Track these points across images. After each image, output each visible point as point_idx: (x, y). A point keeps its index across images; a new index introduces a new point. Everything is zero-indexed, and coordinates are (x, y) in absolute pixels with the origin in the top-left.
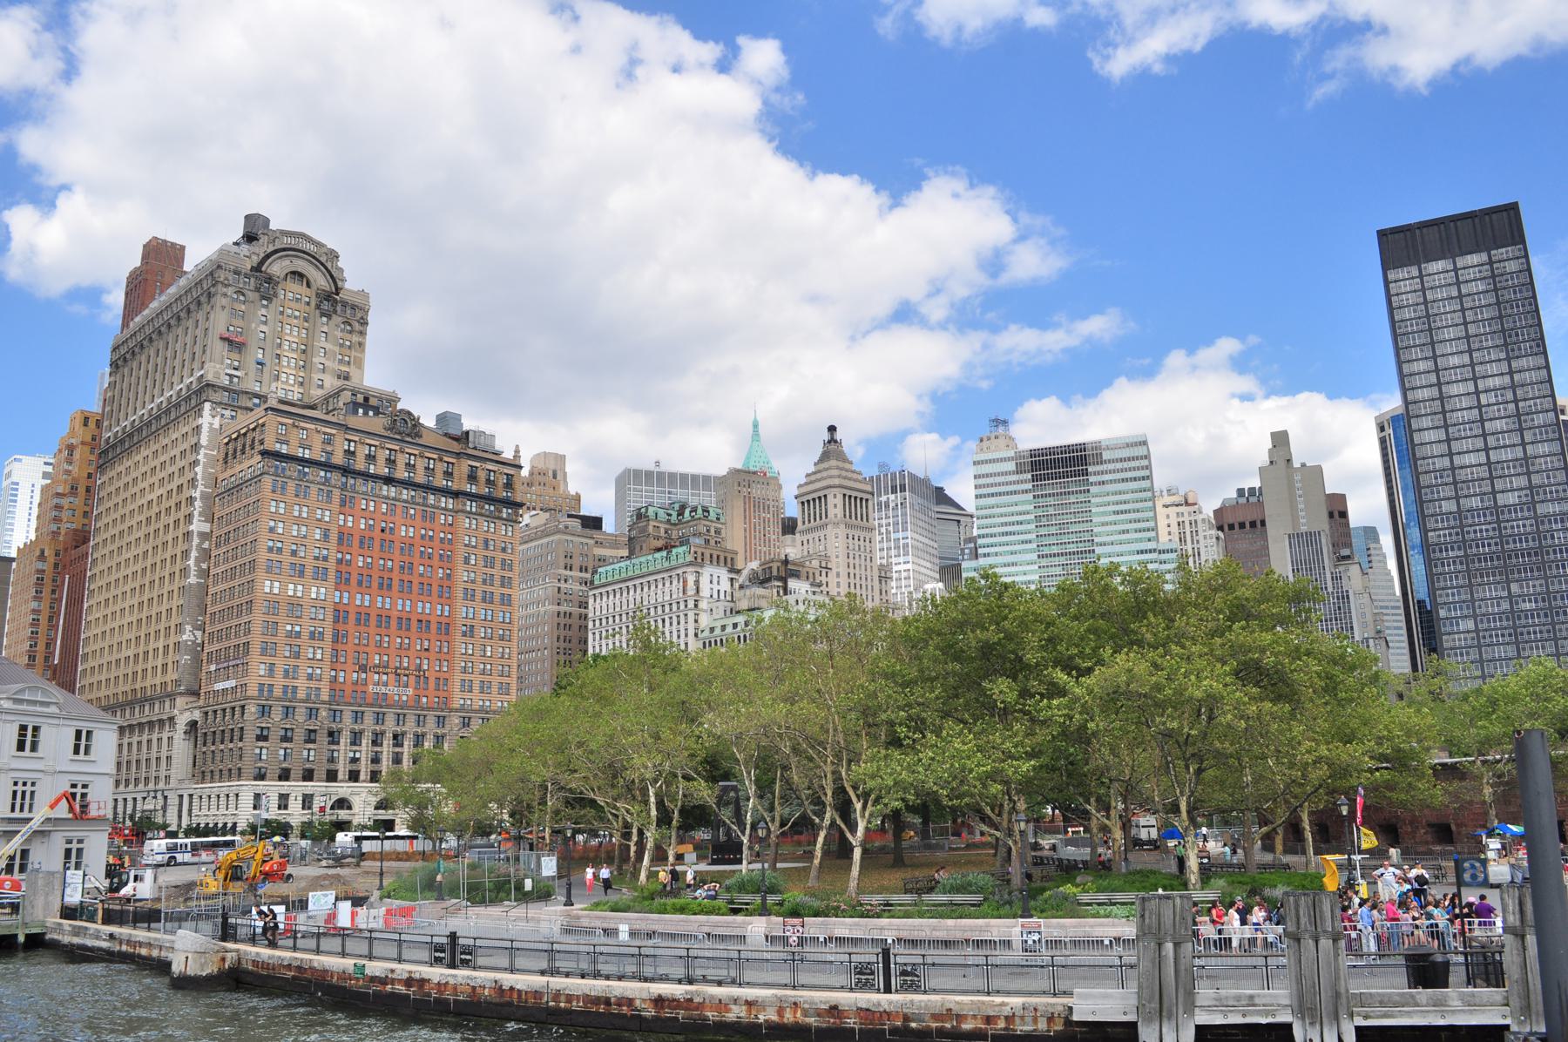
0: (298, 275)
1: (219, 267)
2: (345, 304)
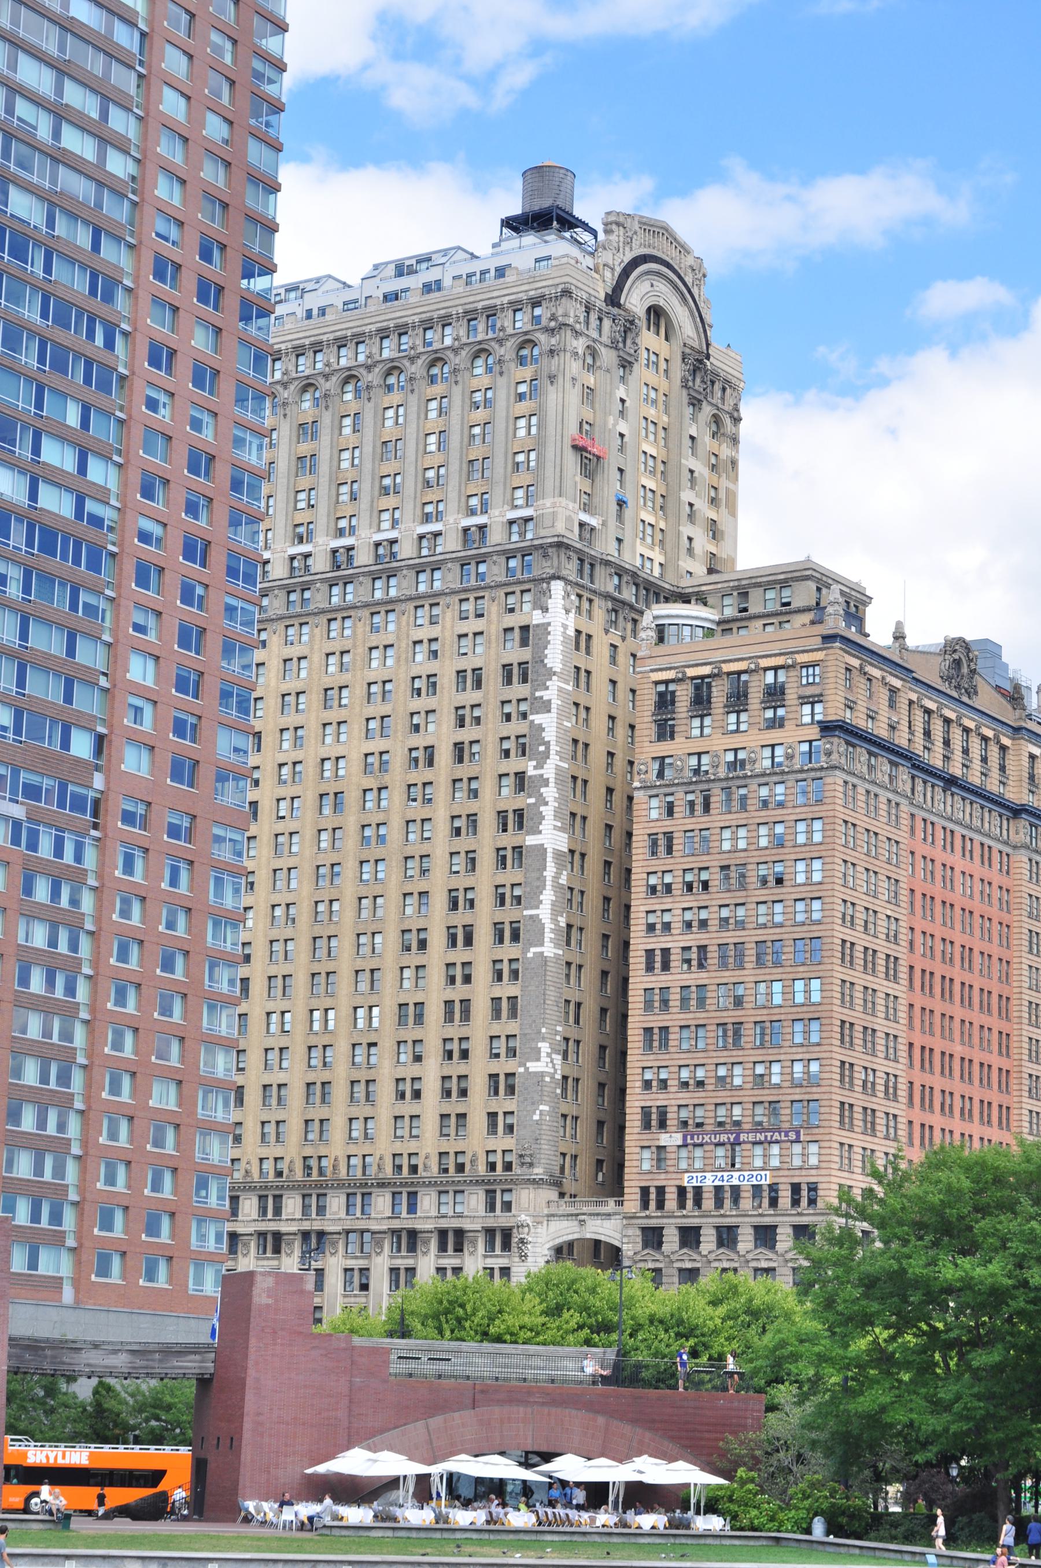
1: (567, 293)
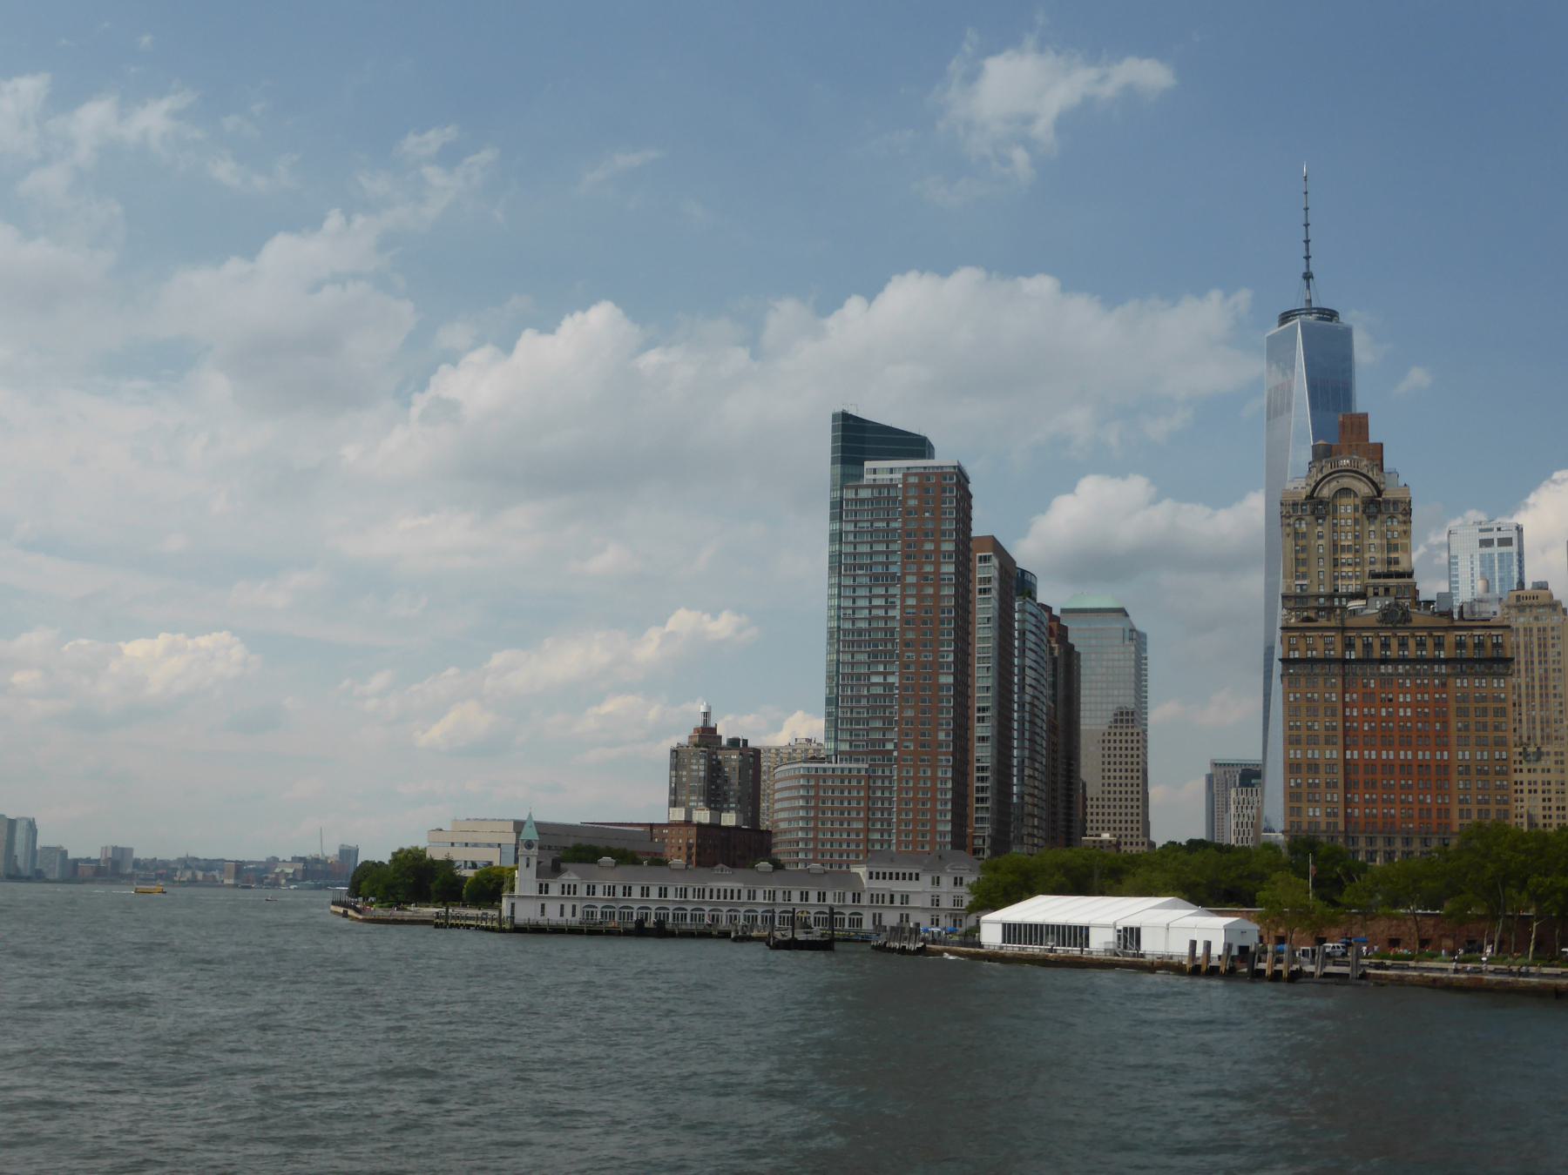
0: (1345, 491)
2: (1387, 502)
